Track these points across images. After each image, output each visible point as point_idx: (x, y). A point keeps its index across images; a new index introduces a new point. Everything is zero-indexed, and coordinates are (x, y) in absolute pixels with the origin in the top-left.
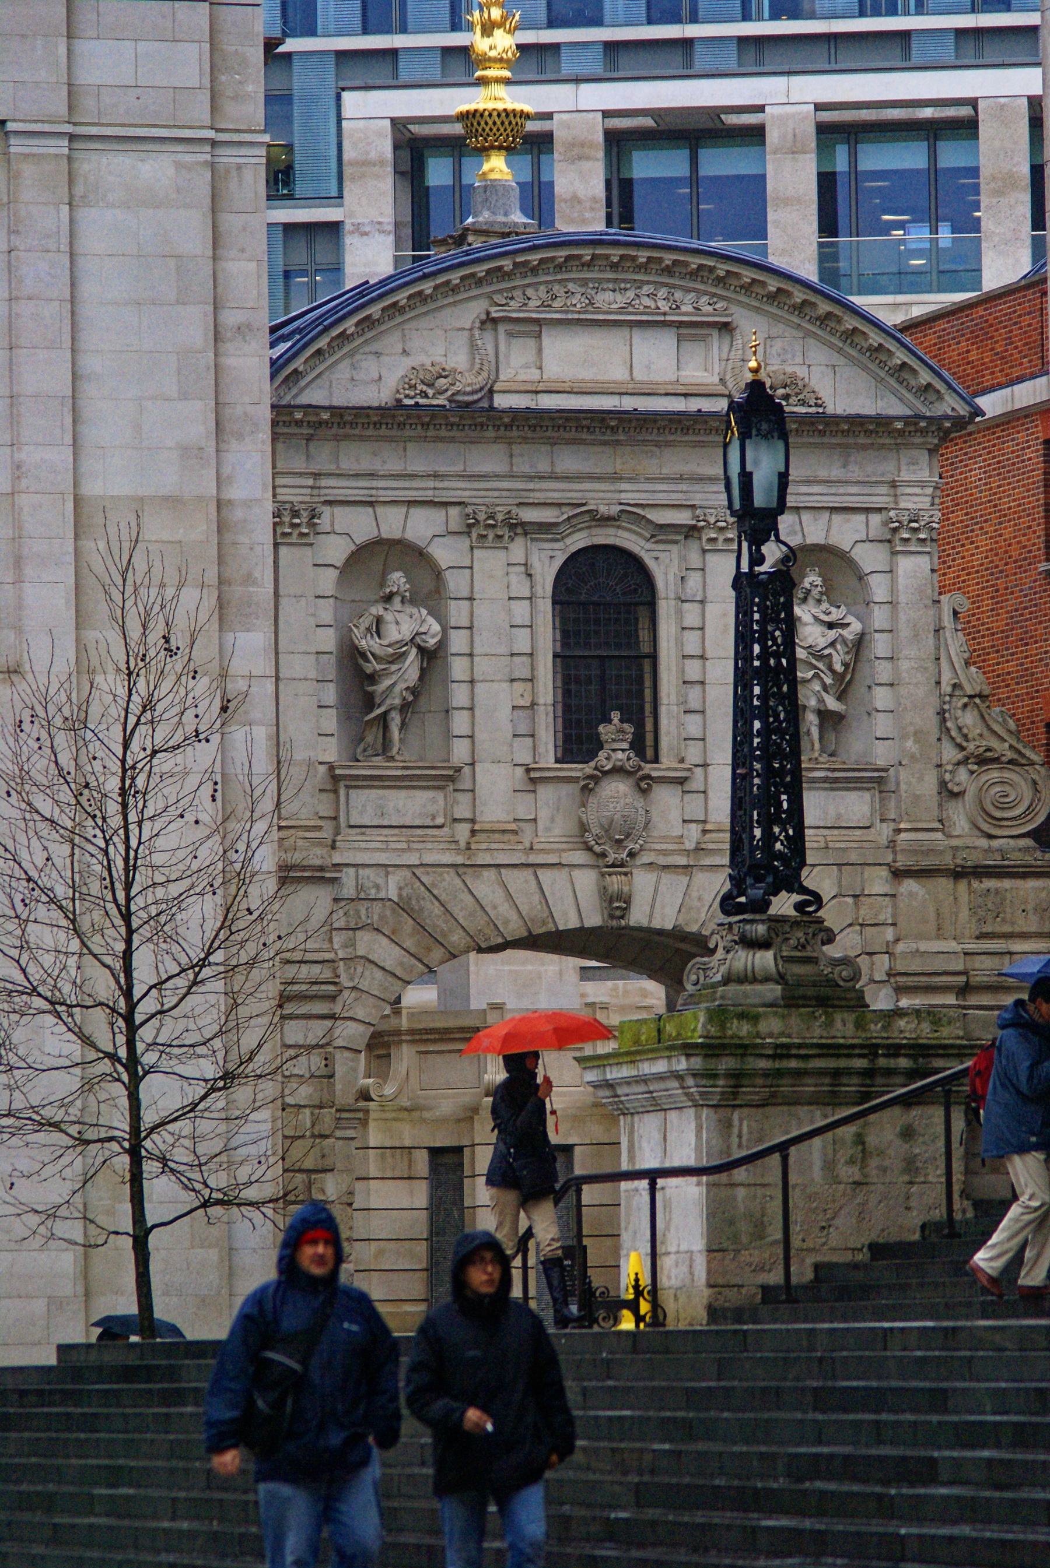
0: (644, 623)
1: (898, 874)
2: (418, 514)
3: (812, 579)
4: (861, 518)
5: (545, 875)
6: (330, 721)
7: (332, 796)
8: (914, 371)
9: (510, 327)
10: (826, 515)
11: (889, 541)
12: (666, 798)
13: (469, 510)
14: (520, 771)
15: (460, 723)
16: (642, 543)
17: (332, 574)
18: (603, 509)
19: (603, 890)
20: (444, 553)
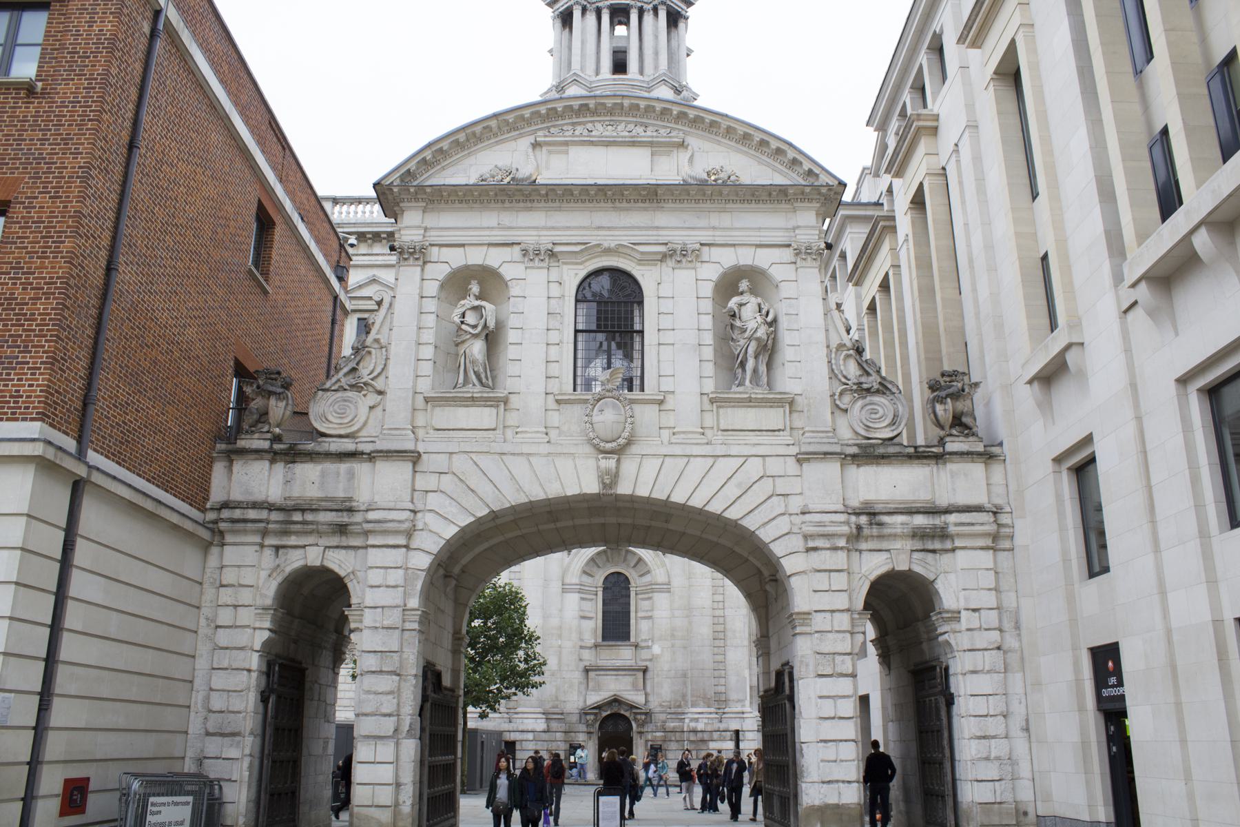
0: (636, 313)
1: (802, 459)
2: (493, 250)
3: (744, 285)
4: (776, 251)
5: (560, 462)
6: (427, 368)
7: (424, 412)
8: (801, 163)
9: (550, 148)
10: (753, 249)
11: (795, 263)
12: (646, 415)
13: (523, 246)
14: (551, 397)
15: (512, 369)
16: (633, 265)
17: (437, 284)
18: (606, 245)
19: (598, 467)
20: (508, 272)
